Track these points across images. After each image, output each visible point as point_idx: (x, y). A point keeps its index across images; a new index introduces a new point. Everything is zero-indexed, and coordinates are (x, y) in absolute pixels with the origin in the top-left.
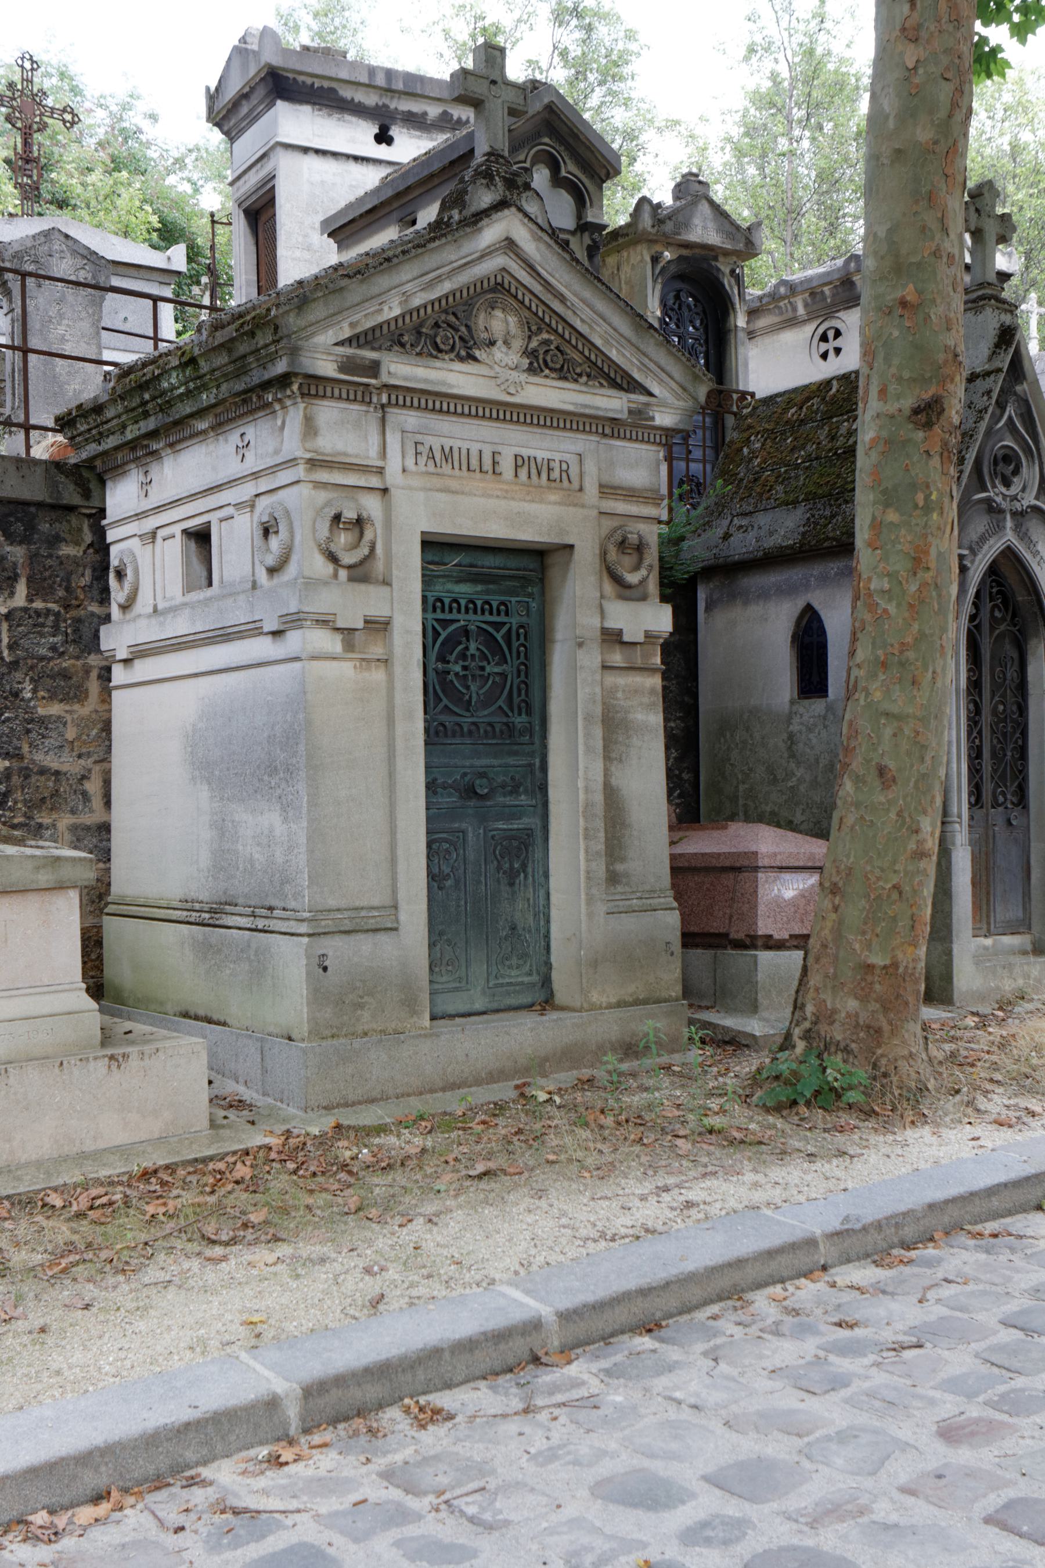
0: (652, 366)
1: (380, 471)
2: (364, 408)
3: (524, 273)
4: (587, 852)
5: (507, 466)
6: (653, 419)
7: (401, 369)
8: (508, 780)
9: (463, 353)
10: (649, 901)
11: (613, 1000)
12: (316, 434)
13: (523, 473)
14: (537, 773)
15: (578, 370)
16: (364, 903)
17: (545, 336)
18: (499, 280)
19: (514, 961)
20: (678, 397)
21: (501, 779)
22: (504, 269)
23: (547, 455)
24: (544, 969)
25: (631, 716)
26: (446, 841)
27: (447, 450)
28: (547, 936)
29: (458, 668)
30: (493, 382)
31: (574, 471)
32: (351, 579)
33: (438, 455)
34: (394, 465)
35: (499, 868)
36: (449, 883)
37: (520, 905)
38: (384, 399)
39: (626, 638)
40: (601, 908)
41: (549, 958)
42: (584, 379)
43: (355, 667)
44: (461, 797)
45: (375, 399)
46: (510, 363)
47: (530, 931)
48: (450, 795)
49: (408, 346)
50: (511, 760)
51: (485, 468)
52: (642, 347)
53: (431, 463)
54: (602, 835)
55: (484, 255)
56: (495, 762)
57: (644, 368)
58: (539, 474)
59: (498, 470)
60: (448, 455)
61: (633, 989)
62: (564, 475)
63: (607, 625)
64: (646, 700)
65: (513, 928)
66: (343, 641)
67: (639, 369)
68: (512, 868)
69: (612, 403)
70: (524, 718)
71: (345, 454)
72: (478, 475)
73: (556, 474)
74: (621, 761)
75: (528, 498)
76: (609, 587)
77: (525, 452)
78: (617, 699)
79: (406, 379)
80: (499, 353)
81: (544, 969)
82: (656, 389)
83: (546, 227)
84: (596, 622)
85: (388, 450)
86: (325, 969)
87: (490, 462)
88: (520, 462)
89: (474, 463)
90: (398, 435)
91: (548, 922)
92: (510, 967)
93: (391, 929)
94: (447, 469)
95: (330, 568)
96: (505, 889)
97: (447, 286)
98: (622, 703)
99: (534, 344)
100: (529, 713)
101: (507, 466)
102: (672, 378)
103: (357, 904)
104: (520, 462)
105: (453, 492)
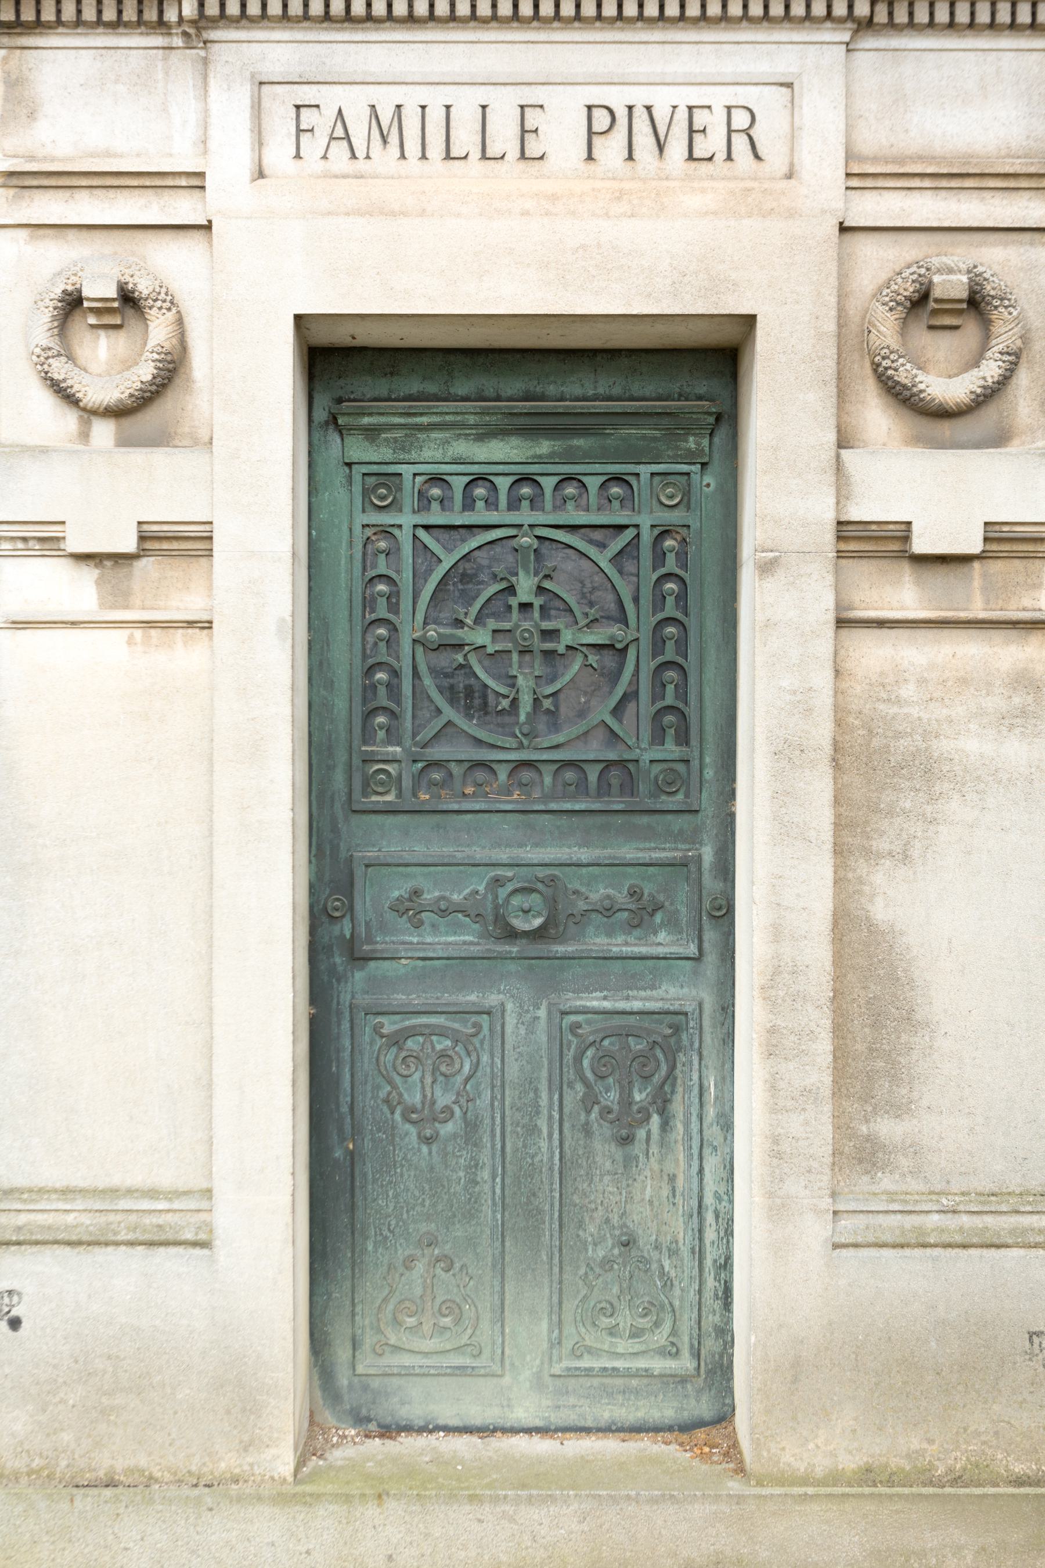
1: (195, 182)
2: (158, 41)
4: (773, 1088)
5: (561, 132)
8: (621, 897)
10: (978, 1221)
11: (849, 1463)
14: (707, 880)
16: (136, 1179)
19: (625, 1319)
21: (598, 893)
24: (711, 1345)
25: (943, 746)
26: (442, 1032)
27: (386, 115)
28: (726, 1264)
29: (481, 637)
32: (124, 441)
34: (227, 166)
35: (590, 1101)
36: (447, 1129)
37: (648, 1187)
39: (920, 546)
40: (814, 1231)
41: (729, 1321)
43: (130, 641)
44: (486, 935)
47: (673, 1252)
48: (457, 928)
50: (629, 852)
53: (340, 150)
54: (823, 1047)
56: (584, 855)
58: (661, 147)
59: (533, 148)
60: (386, 129)
61: (900, 1445)
62: (740, 143)
63: (855, 513)
64: (995, 703)
65: (628, 1244)
66: (99, 582)
68: (626, 1101)
70: (671, 749)
71: (108, 154)
73: (713, 143)
74: (905, 857)
76: (877, 417)
77: (617, 98)
78: (898, 701)
81: (711, 1345)
84: (822, 511)
85: (214, 132)
86: (15, 1324)
87: (513, 130)
88: (601, 120)
89: (465, 139)
90: (244, 94)
91: (729, 1233)
92: (612, 1331)
93: (195, 1244)
94: (385, 158)
95: (71, 420)
96: (604, 1151)
98: (915, 711)
100: (683, 738)
101: (561, 132)
103: (117, 1180)
104: (601, 120)
105: (393, 214)
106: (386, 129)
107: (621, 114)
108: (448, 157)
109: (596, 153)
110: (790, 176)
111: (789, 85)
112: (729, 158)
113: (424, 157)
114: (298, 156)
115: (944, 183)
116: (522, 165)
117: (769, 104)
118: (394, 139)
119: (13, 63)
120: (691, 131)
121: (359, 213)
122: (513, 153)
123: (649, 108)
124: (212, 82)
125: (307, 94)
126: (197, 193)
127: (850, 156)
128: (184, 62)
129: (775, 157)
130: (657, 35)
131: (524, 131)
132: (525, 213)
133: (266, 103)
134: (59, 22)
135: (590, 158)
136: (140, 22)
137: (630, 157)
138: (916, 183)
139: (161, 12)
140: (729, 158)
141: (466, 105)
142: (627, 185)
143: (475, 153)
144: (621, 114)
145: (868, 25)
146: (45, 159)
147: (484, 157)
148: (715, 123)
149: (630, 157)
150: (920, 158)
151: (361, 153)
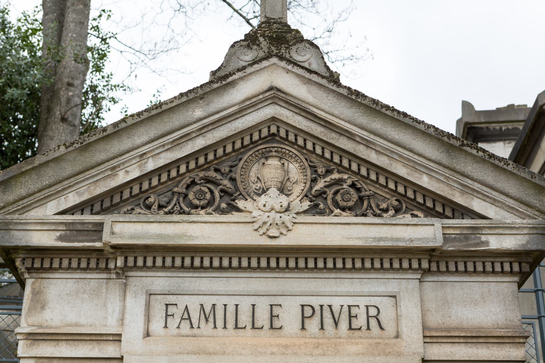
0: (476, 186)
1: (117, 338)
2: (105, 276)
3: (300, 118)
5: (289, 317)
6: (487, 243)
7: (126, 229)
9: (224, 205)
12: (43, 308)
13: (313, 325)
15: (384, 206)
17: (336, 176)
18: (273, 130)
20: (522, 215)
22: (274, 119)
23: (348, 301)
27: (208, 309)
30: (250, 227)
31: (387, 316)
33: (195, 315)
38: (120, 262)
42: (392, 212)
45: (112, 265)
46: (278, 208)
49: (155, 207)
51: (258, 324)
52: (458, 167)
53: (185, 325)
55: (243, 109)
57: (467, 190)
58: (336, 324)
59: (277, 324)
60: (208, 315)
62: (373, 322)
67: (463, 193)
69: (425, 232)
71: (77, 325)
72: (249, 331)
73: (361, 321)
75: (319, 351)
77: (315, 302)
79: (131, 237)
80: (273, 199)
82: (477, 205)
83: (323, 71)
85: (127, 316)
87: (267, 316)
88: (308, 312)
89: (245, 319)
90: (142, 300)
94: (207, 329)
97: (200, 143)
99: (320, 185)
101: (289, 317)
102: (507, 195)
105: (210, 354)
106: (208, 315)
107: (317, 309)
108: (236, 327)
109: (306, 326)
110: (397, 337)
111: (395, 297)
112: (368, 328)
113: (225, 327)
114: (166, 327)
115: (470, 340)
116: (271, 331)
117: (385, 304)
118: (211, 319)
119: (37, 285)
120: (350, 317)
121: (194, 353)
122: (267, 325)
123: (330, 306)
124: (128, 294)
125: (172, 299)
126: (117, 343)
127: (425, 328)
128: (115, 286)
129: (390, 329)
130: (333, 275)
131: (272, 316)
132: (273, 354)
133: (152, 303)
134: (60, 268)
135: (303, 328)
136: (97, 268)
137: (322, 328)
138: (457, 340)
139: (107, 264)
140: (368, 328)
141: (245, 304)
142: (321, 341)
143: (249, 326)
144: (317, 309)
145: (428, 271)
146: (47, 327)
147: (253, 327)
148: (361, 313)
149: (322, 328)
150: (457, 329)
151: (195, 325)
